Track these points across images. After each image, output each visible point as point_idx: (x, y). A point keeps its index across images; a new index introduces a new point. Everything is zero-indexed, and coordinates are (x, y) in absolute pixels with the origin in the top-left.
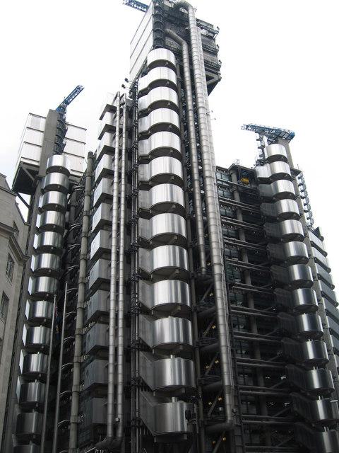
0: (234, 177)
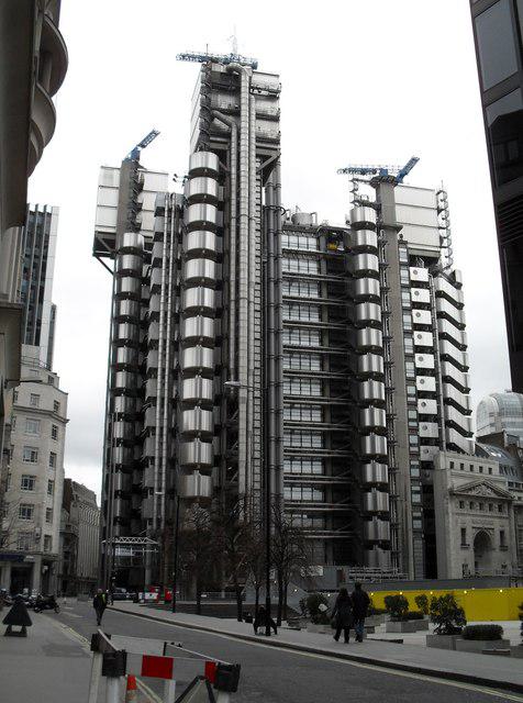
0: (323, 240)
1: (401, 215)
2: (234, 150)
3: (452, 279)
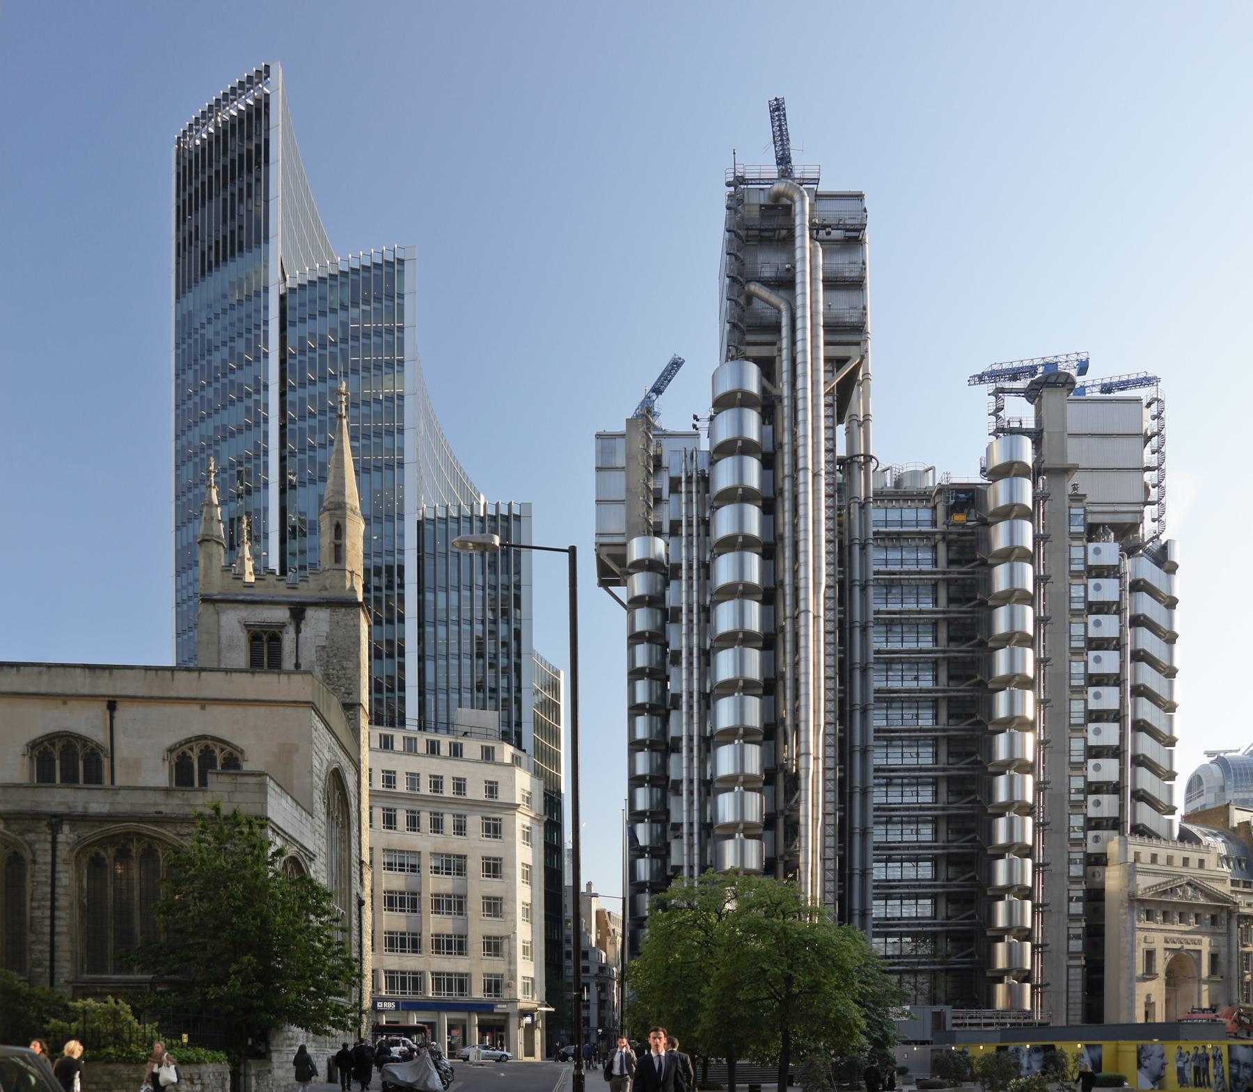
1: (1075, 453)
2: (785, 353)
3: (1162, 558)
